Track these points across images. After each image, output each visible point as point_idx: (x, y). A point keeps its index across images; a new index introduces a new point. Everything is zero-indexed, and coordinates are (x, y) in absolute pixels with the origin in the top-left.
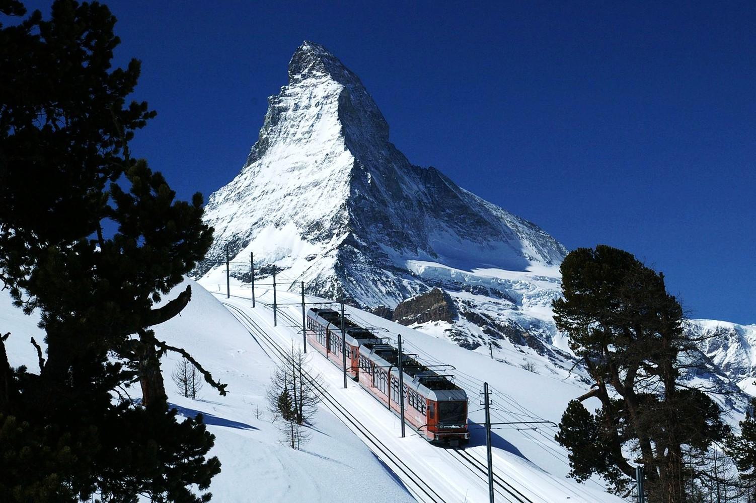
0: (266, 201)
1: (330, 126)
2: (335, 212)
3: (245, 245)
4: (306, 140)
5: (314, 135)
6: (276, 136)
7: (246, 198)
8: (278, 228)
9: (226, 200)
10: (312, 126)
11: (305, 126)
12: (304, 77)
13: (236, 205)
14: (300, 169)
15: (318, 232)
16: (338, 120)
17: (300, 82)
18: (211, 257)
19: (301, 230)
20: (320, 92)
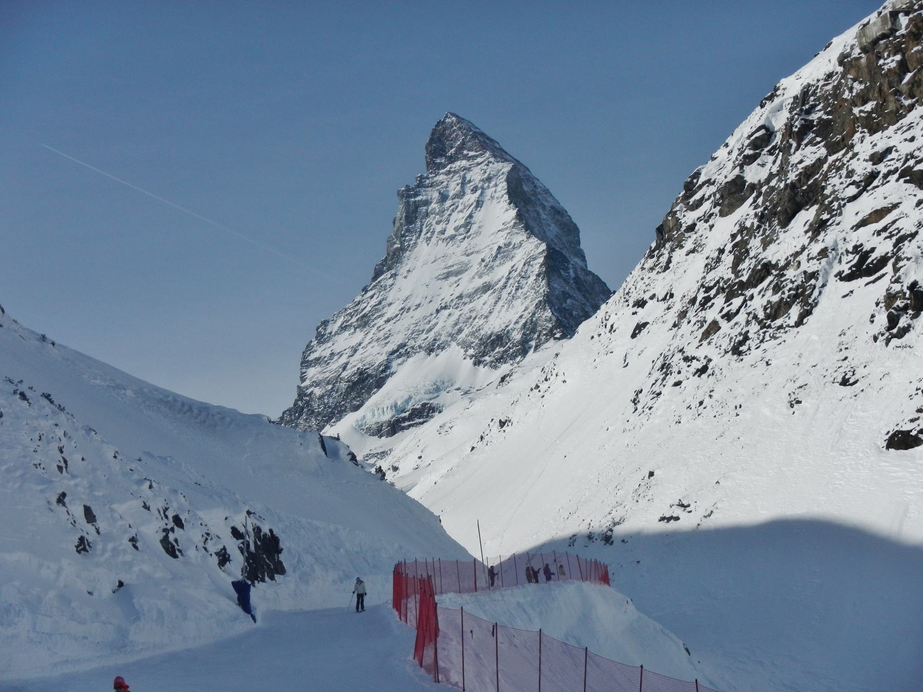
0: (407, 321)
1: (500, 213)
2: (527, 315)
3: (380, 383)
4: (463, 236)
5: (474, 228)
6: (414, 238)
7: (376, 321)
8: (433, 354)
9: (343, 328)
10: (470, 216)
11: (458, 218)
12: (452, 159)
13: (359, 336)
14: (458, 273)
15: (502, 349)
16: (510, 204)
17: (445, 166)
18: (325, 408)
19: (471, 352)
20: (476, 175)
